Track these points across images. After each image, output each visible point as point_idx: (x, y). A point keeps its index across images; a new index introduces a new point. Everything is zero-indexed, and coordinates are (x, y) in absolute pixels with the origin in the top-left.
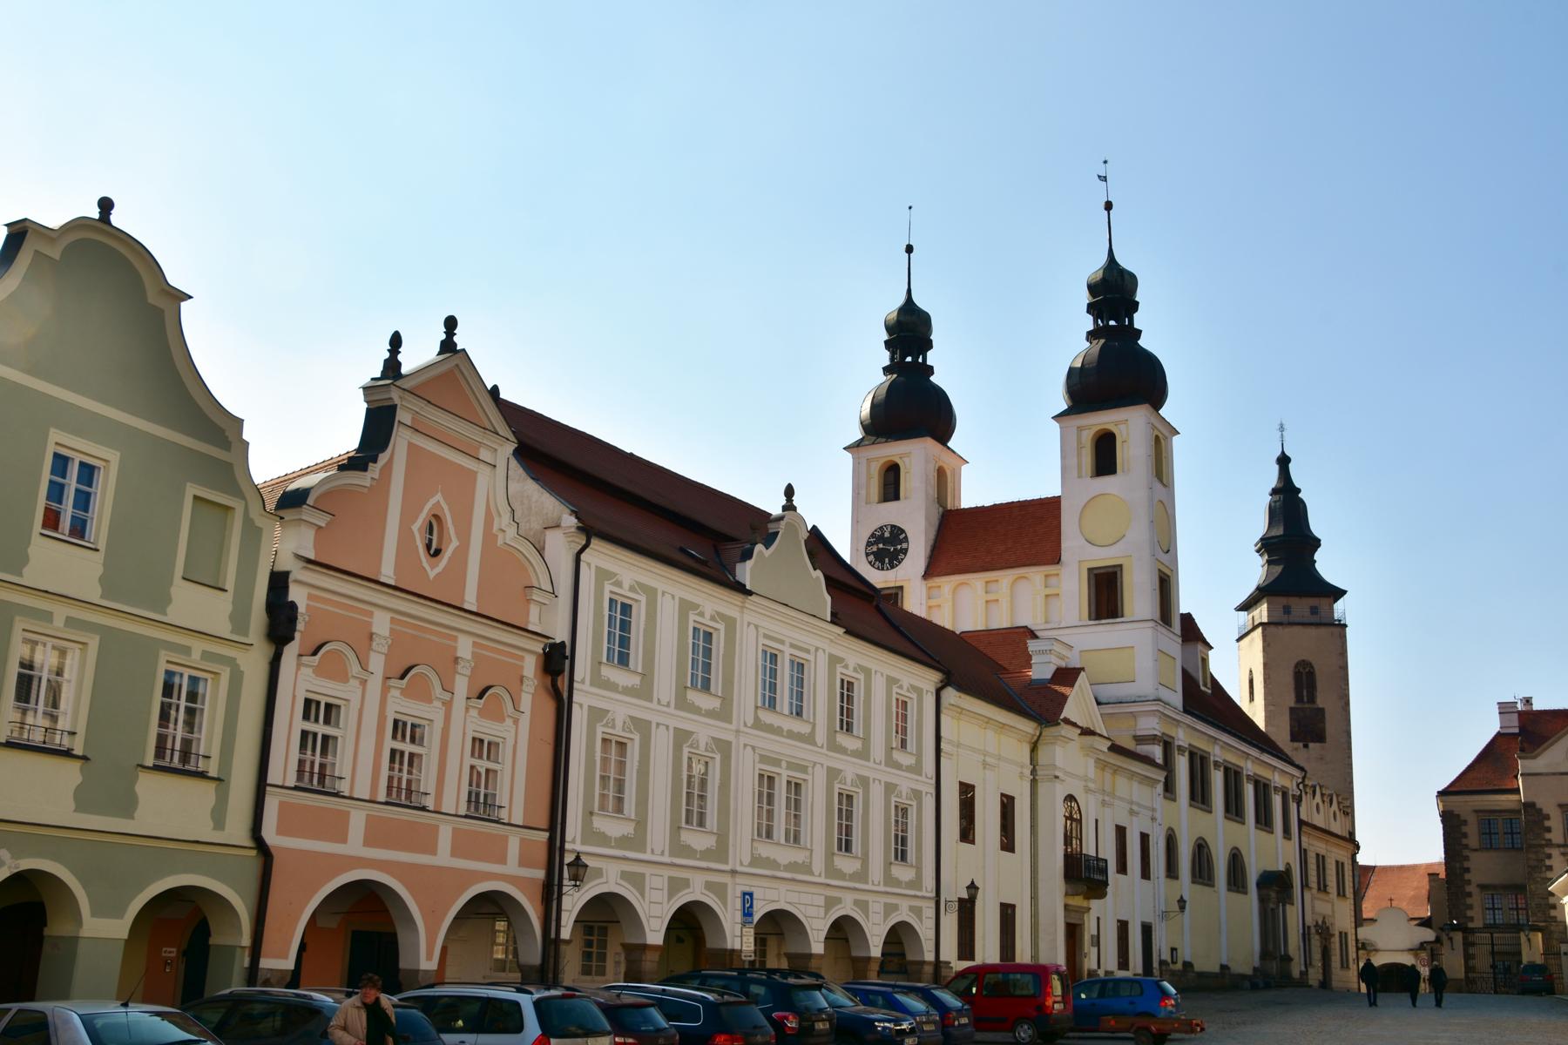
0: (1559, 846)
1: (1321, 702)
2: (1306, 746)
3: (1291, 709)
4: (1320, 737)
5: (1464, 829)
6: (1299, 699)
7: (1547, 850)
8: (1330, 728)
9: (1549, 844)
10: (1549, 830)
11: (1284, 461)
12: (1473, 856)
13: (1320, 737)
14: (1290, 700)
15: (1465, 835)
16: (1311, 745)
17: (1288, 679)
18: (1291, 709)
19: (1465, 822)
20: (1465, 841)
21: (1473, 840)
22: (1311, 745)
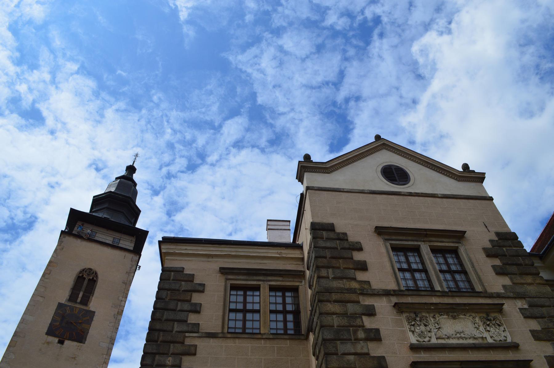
0: (387, 293)
1: (93, 305)
2: (61, 342)
3: (60, 305)
4: (80, 337)
5: (196, 298)
6: (73, 297)
7: (368, 301)
8: (95, 331)
9: (366, 290)
10: (363, 267)
11: (131, 169)
12: (203, 345)
13: (80, 337)
14: (63, 296)
15: (197, 309)
16: (67, 342)
17: (69, 280)
18: (60, 305)
19: (201, 289)
20: (193, 318)
21: (210, 316)
22: (67, 342)
